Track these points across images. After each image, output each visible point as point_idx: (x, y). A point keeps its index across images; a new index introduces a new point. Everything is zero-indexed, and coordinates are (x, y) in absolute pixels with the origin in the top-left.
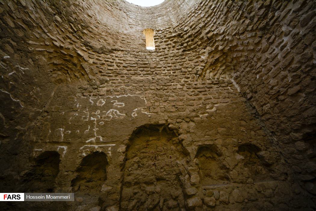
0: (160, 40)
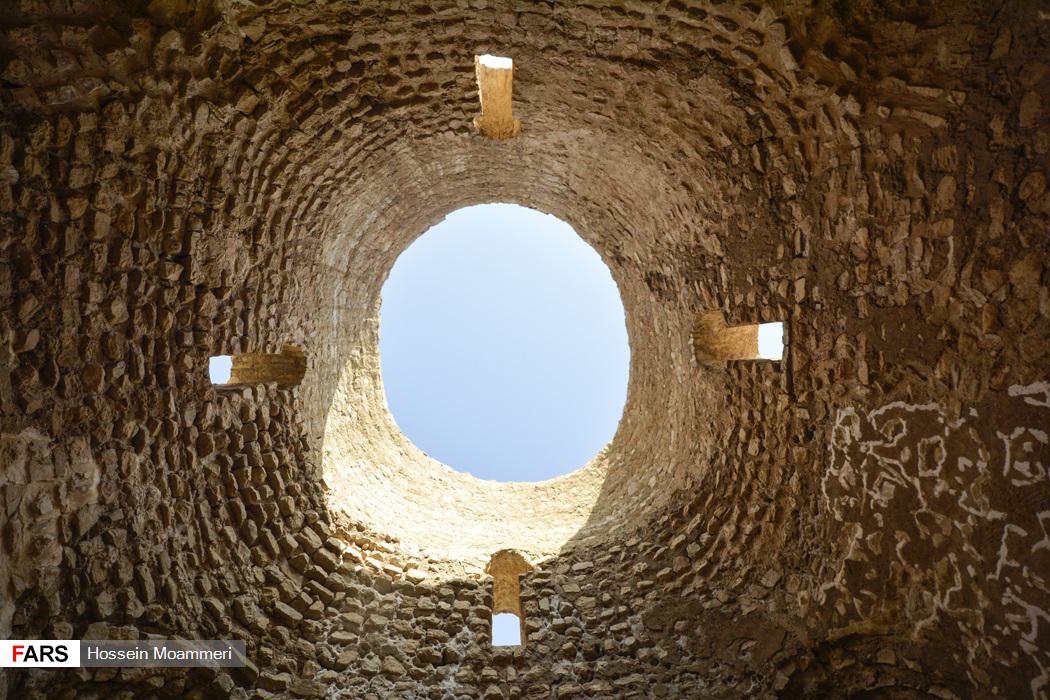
0: (457, 93)
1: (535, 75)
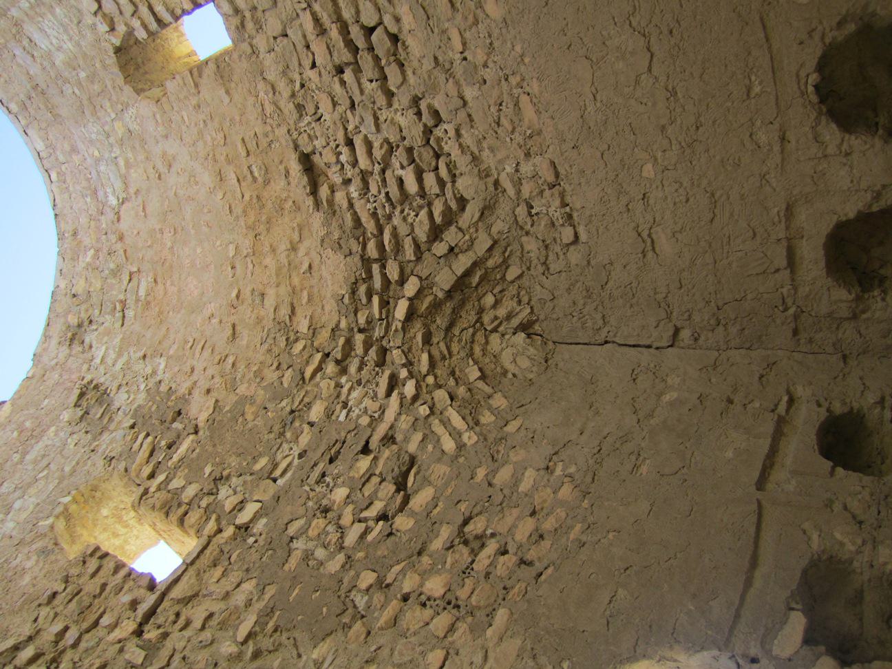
1: (233, 85)
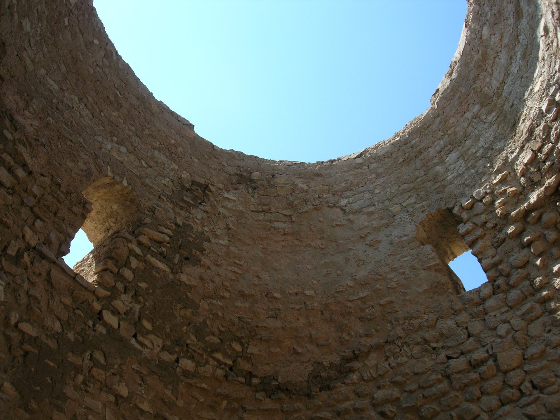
1: (431, 295)
